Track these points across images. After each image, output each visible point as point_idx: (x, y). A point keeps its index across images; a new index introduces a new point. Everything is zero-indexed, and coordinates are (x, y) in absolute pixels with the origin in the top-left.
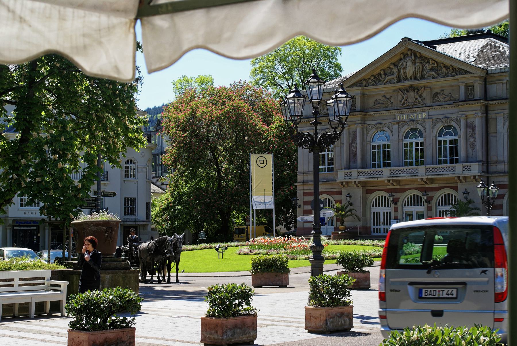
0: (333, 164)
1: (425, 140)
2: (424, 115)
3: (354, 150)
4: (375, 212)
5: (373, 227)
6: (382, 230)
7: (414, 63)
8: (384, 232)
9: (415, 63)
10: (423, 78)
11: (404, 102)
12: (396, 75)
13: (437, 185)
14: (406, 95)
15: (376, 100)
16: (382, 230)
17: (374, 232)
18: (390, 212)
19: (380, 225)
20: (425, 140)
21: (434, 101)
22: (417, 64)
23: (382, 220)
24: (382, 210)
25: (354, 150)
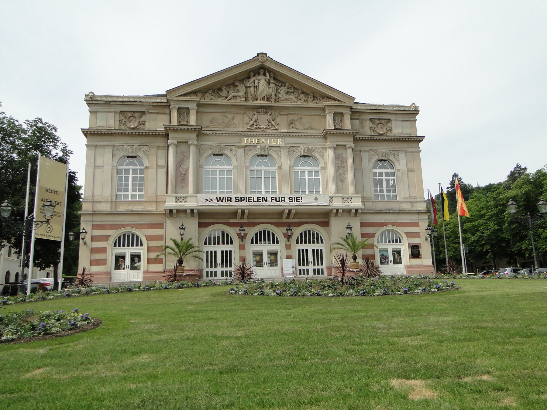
0: (141, 190)
1: (280, 168)
2: (279, 142)
3: (184, 173)
4: (209, 250)
5: (205, 270)
6: (219, 274)
7: (269, 83)
10: (277, 100)
11: (253, 124)
12: (242, 94)
13: (297, 220)
14: (256, 116)
15: (214, 119)
16: (219, 274)
17: (207, 276)
18: (230, 252)
19: (215, 267)
20: (280, 168)
21: (290, 127)
22: (272, 85)
23: (219, 260)
24: (219, 248)
25: (184, 173)
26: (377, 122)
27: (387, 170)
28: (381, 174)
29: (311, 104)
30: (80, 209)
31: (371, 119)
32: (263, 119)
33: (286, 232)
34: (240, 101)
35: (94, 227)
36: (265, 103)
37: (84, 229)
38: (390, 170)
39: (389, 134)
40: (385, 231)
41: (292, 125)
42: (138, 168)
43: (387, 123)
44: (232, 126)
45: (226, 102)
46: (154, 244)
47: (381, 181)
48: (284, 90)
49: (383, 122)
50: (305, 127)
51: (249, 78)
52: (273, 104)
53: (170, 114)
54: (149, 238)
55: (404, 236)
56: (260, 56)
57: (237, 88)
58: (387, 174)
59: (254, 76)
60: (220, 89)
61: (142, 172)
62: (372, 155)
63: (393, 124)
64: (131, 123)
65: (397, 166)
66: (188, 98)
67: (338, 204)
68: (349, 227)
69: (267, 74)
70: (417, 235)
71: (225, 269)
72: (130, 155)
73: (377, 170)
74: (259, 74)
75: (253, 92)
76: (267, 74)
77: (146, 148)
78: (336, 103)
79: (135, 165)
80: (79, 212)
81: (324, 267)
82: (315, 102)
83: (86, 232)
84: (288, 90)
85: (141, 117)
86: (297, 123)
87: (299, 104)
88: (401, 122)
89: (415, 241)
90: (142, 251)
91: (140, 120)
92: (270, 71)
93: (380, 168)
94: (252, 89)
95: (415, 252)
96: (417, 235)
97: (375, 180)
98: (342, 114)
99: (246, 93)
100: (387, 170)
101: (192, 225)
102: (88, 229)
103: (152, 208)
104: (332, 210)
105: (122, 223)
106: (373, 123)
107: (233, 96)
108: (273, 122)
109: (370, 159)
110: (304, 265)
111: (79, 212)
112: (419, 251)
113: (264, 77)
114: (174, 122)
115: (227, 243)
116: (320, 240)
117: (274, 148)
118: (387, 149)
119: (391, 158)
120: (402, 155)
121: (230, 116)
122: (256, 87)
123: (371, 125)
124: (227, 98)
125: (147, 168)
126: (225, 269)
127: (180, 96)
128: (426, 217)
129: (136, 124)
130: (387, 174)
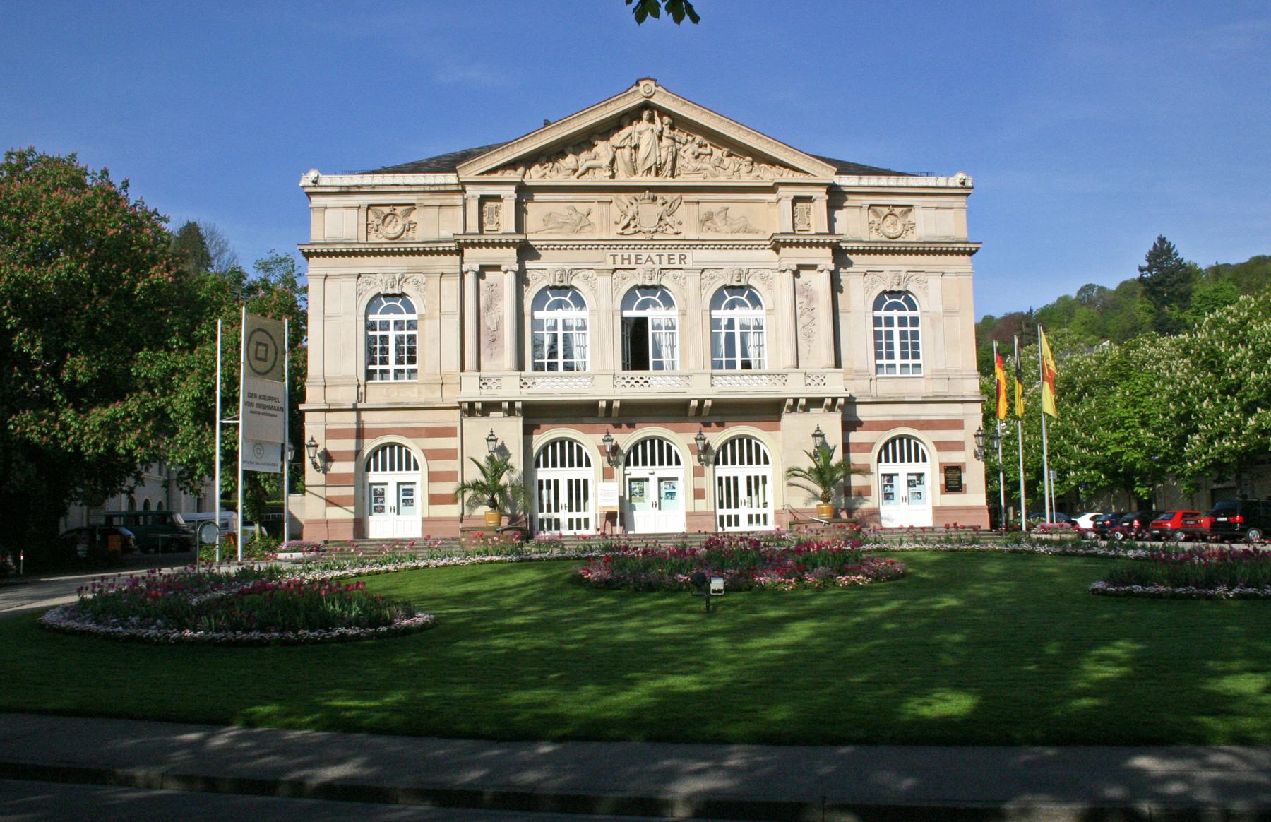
1: (683, 313)
3: (493, 327)
6: (564, 522)
8: (571, 528)
9: (660, 138)
11: (628, 225)
18: (586, 481)
19: (557, 510)
22: (666, 142)
23: (563, 498)
24: (563, 475)
26: (886, 211)
27: (902, 314)
28: (889, 322)
29: (747, 180)
30: (303, 400)
31: (871, 206)
32: (649, 212)
33: (694, 442)
34: (601, 178)
35: (331, 434)
36: (651, 180)
37: (312, 440)
38: (908, 314)
39: (910, 237)
40: (893, 440)
41: (708, 224)
42: (406, 317)
43: (905, 214)
44: (588, 229)
45: (573, 181)
46: (440, 466)
47: (889, 335)
48: (690, 151)
49: (897, 211)
50: (736, 227)
51: (620, 127)
52: (670, 182)
53: (464, 205)
54: (431, 455)
55: (933, 448)
56: (642, 83)
57: (595, 150)
58: (902, 322)
59: (631, 124)
60: (564, 156)
61: (412, 325)
62: (874, 282)
63: (917, 216)
64: (390, 228)
65: (923, 304)
66: (497, 177)
67: (795, 388)
68: (818, 434)
69: (657, 118)
70: (958, 446)
71: (575, 515)
72: (390, 291)
73: (882, 314)
74: (640, 119)
75: (627, 159)
76: (657, 118)
77: (419, 277)
78: (799, 178)
79: (399, 311)
80: (302, 407)
81: (770, 511)
82: (754, 174)
83: (316, 446)
84: (701, 150)
85: (408, 214)
86: (716, 219)
87: (722, 180)
88: (933, 212)
89: (954, 458)
90: (418, 478)
91: (406, 221)
92: (663, 112)
93: (889, 308)
94: (627, 152)
95: (953, 481)
96: (958, 446)
97: (877, 335)
98: (809, 199)
99: (613, 161)
100: (902, 314)
101: (510, 430)
102: (320, 440)
103: (434, 397)
104: (785, 399)
105: (380, 426)
106: (877, 215)
107: (588, 169)
108: (668, 219)
109: (867, 290)
110: (729, 507)
111: (302, 407)
112: (960, 478)
113: (651, 126)
114: (473, 226)
115: (580, 465)
116: (759, 457)
117: (672, 272)
118: (904, 269)
119: (911, 287)
120: (934, 282)
121: (583, 208)
122: (636, 147)
123: (872, 217)
124: (575, 171)
125: (422, 317)
126: (575, 515)
127: (483, 174)
128: (978, 408)
129: (399, 229)
130: (902, 322)
